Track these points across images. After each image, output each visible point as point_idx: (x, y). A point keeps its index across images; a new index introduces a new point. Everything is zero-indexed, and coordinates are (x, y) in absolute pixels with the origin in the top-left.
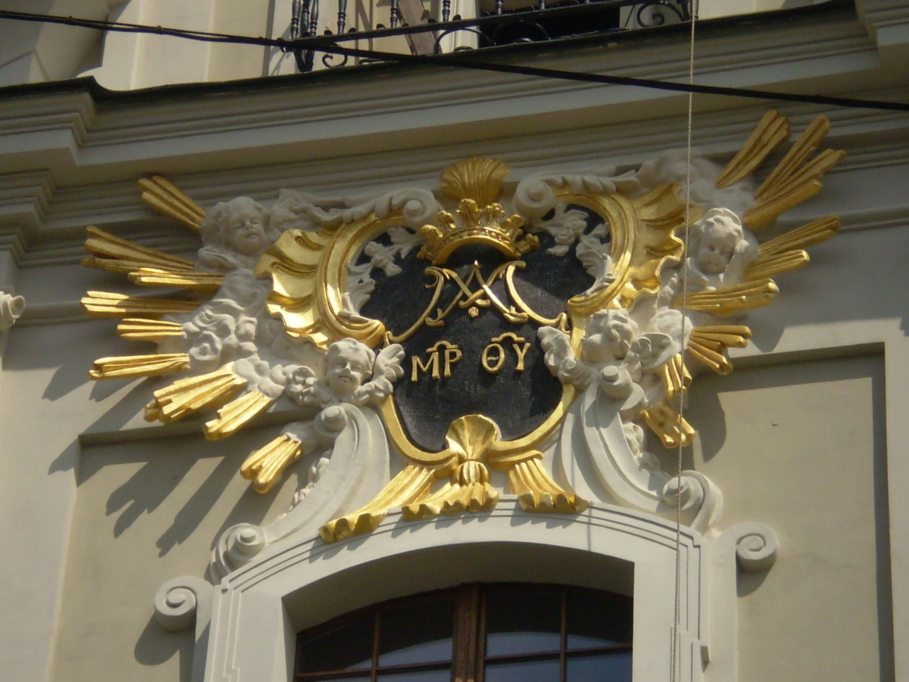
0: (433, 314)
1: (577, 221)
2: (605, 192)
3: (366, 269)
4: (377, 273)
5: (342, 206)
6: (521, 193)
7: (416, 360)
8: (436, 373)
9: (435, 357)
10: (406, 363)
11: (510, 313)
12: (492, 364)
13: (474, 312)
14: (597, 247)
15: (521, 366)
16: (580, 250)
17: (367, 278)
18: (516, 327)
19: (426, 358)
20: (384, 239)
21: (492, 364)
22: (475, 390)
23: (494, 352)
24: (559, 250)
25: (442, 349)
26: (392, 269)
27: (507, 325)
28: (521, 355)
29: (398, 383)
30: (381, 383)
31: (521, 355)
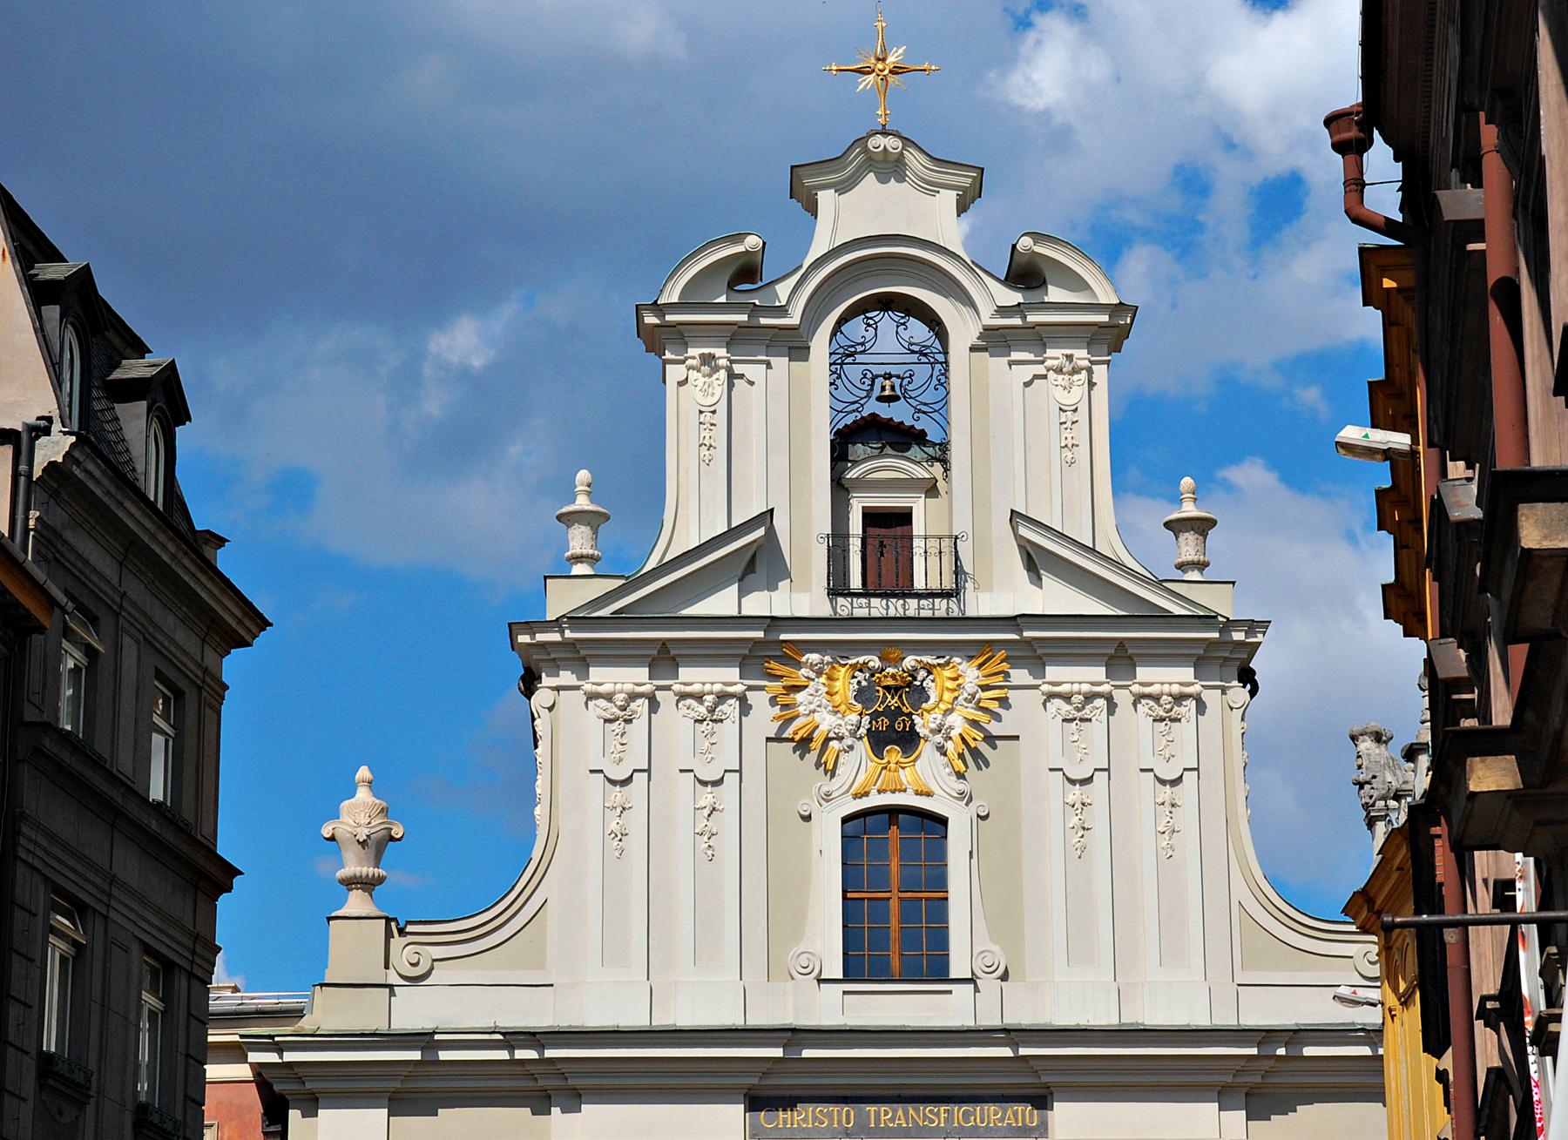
0: (879, 706)
2: (934, 666)
3: (855, 680)
4: (859, 682)
5: (847, 658)
7: (874, 722)
8: (880, 729)
9: (880, 723)
10: (870, 723)
11: (904, 709)
12: (899, 728)
13: (893, 708)
14: (931, 684)
15: (907, 729)
16: (924, 685)
17: (855, 685)
18: (906, 715)
19: (877, 722)
20: (861, 671)
21: (899, 728)
23: (899, 723)
24: (918, 683)
25: (883, 720)
26: (864, 683)
27: (903, 714)
28: (908, 725)
29: (868, 730)
30: (863, 731)
31: (908, 725)
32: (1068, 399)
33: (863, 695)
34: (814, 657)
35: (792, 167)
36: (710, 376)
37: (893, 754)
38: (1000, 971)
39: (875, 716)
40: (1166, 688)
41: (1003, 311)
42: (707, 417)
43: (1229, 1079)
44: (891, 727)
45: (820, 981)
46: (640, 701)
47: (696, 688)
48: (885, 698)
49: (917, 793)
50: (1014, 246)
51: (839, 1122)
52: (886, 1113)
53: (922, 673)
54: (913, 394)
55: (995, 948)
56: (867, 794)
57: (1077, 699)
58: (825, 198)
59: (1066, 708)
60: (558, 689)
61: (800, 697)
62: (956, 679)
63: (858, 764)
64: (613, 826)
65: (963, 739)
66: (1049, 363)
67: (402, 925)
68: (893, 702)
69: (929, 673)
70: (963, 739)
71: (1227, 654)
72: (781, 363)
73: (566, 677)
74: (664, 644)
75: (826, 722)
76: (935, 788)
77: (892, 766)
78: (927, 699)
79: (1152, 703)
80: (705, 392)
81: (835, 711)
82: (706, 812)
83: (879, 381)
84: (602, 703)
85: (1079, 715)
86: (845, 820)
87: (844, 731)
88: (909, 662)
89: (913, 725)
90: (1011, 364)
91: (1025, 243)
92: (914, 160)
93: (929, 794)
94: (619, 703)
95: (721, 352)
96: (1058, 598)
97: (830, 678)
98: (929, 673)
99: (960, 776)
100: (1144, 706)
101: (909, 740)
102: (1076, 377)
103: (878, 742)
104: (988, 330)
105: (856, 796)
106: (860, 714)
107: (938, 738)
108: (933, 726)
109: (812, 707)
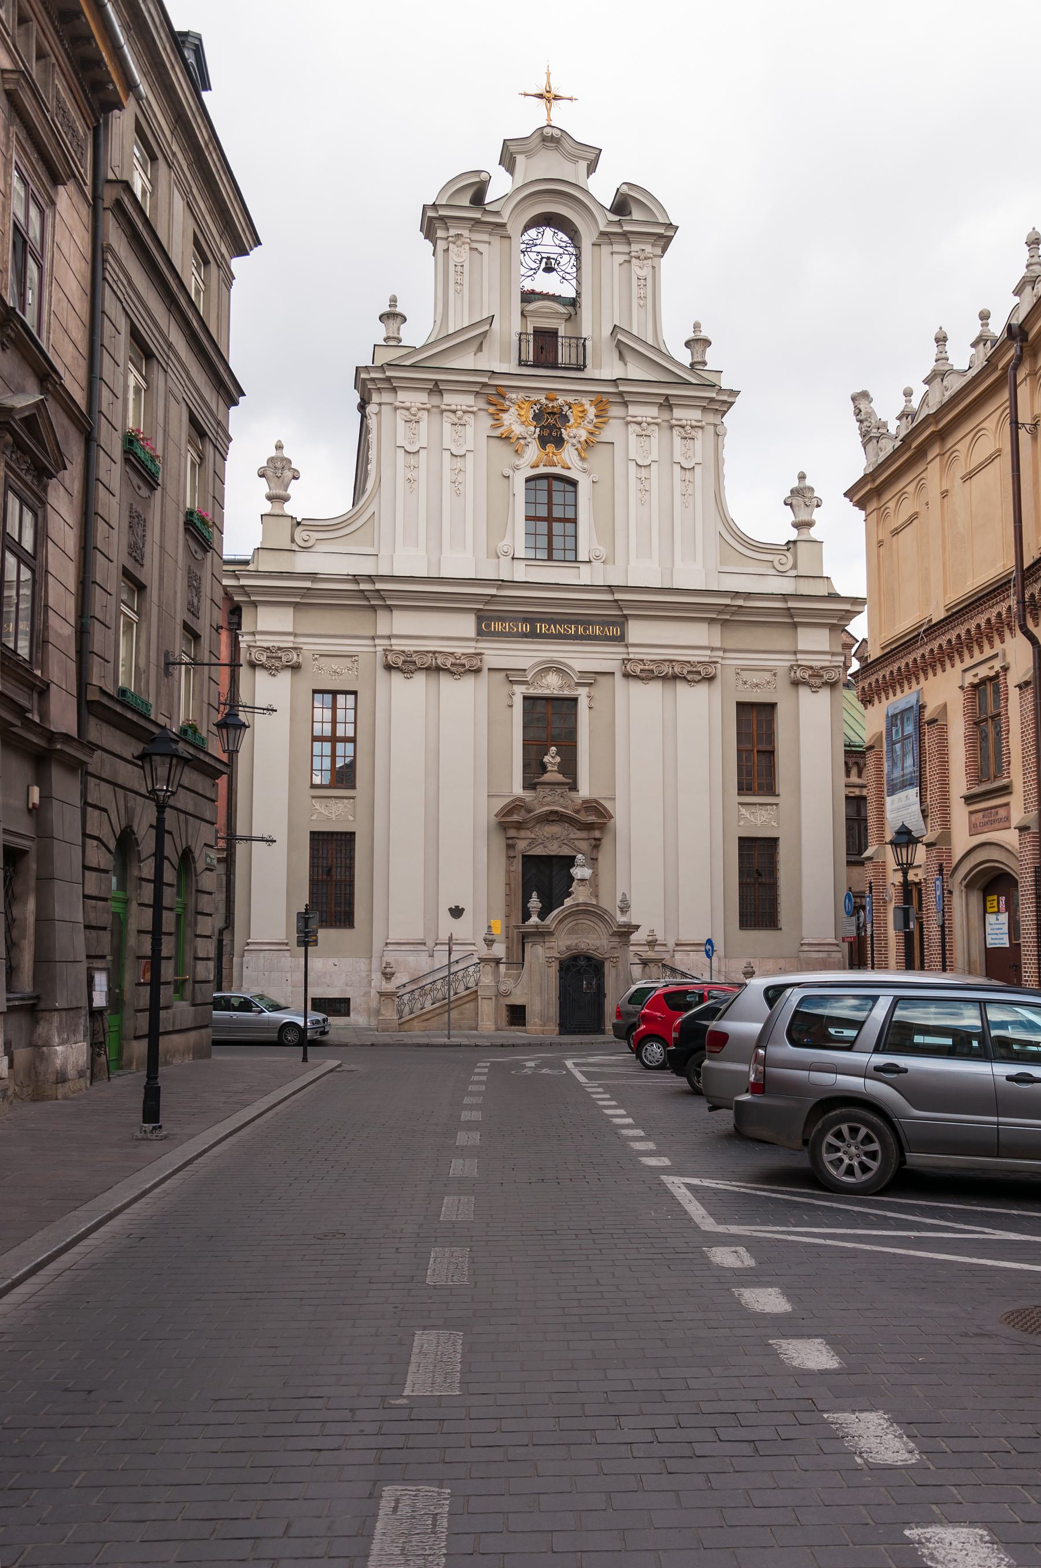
1: (567, 408)
6: (559, 401)
22: (552, 439)
30: (536, 435)
32: (642, 273)
33: (537, 417)
34: (514, 396)
35: (505, 140)
36: (461, 247)
37: (550, 448)
38: (602, 560)
39: (542, 428)
40: (689, 422)
41: (610, 223)
42: (459, 269)
43: (714, 616)
44: (550, 434)
45: (513, 558)
46: (422, 412)
47: (453, 407)
48: (548, 419)
49: (563, 467)
50: (618, 189)
51: (522, 629)
52: (545, 627)
53: (566, 408)
54: (563, 268)
55: (601, 548)
56: (538, 466)
57: (644, 425)
58: (520, 159)
59: (637, 428)
60: (380, 404)
61: (505, 416)
62: (583, 412)
63: (533, 451)
64: (409, 476)
65: (586, 442)
66: (633, 254)
67: (299, 520)
68: (551, 421)
69: (570, 408)
70: (586, 442)
71: (717, 407)
72: (496, 241)
73: (386, 397)
74: (436, 384)
75: (518, 429)
76: (570, 465)
77: (551, 455)
78: (569, 421)
79: (681, 430)
80: (458, 256)
81: (523, 423)
82: (457, 471)
83: (544, 260)
84: (403, 412)
85: (644, 433)
86: (528, 480)
87: (526, 435)
88: (561, 400)
89: (561, 434)
90: (612, 253)
91: (625, 188)
92: (566, 144)
93: (569, 468)
94: (413, 412)
95: (466, 233)
96: (635, 371)
97: (520, 407)
98: (570, 408)
99: (583, 459)
100: (676, 431)
101: (559, 442)
102: (645, 262)
103: (543, 441)
104: (603, 234)
105: (532, 467)
106: (535, 427)
107: (574, 441)
108: (572, 435)
109: (511, 421)
